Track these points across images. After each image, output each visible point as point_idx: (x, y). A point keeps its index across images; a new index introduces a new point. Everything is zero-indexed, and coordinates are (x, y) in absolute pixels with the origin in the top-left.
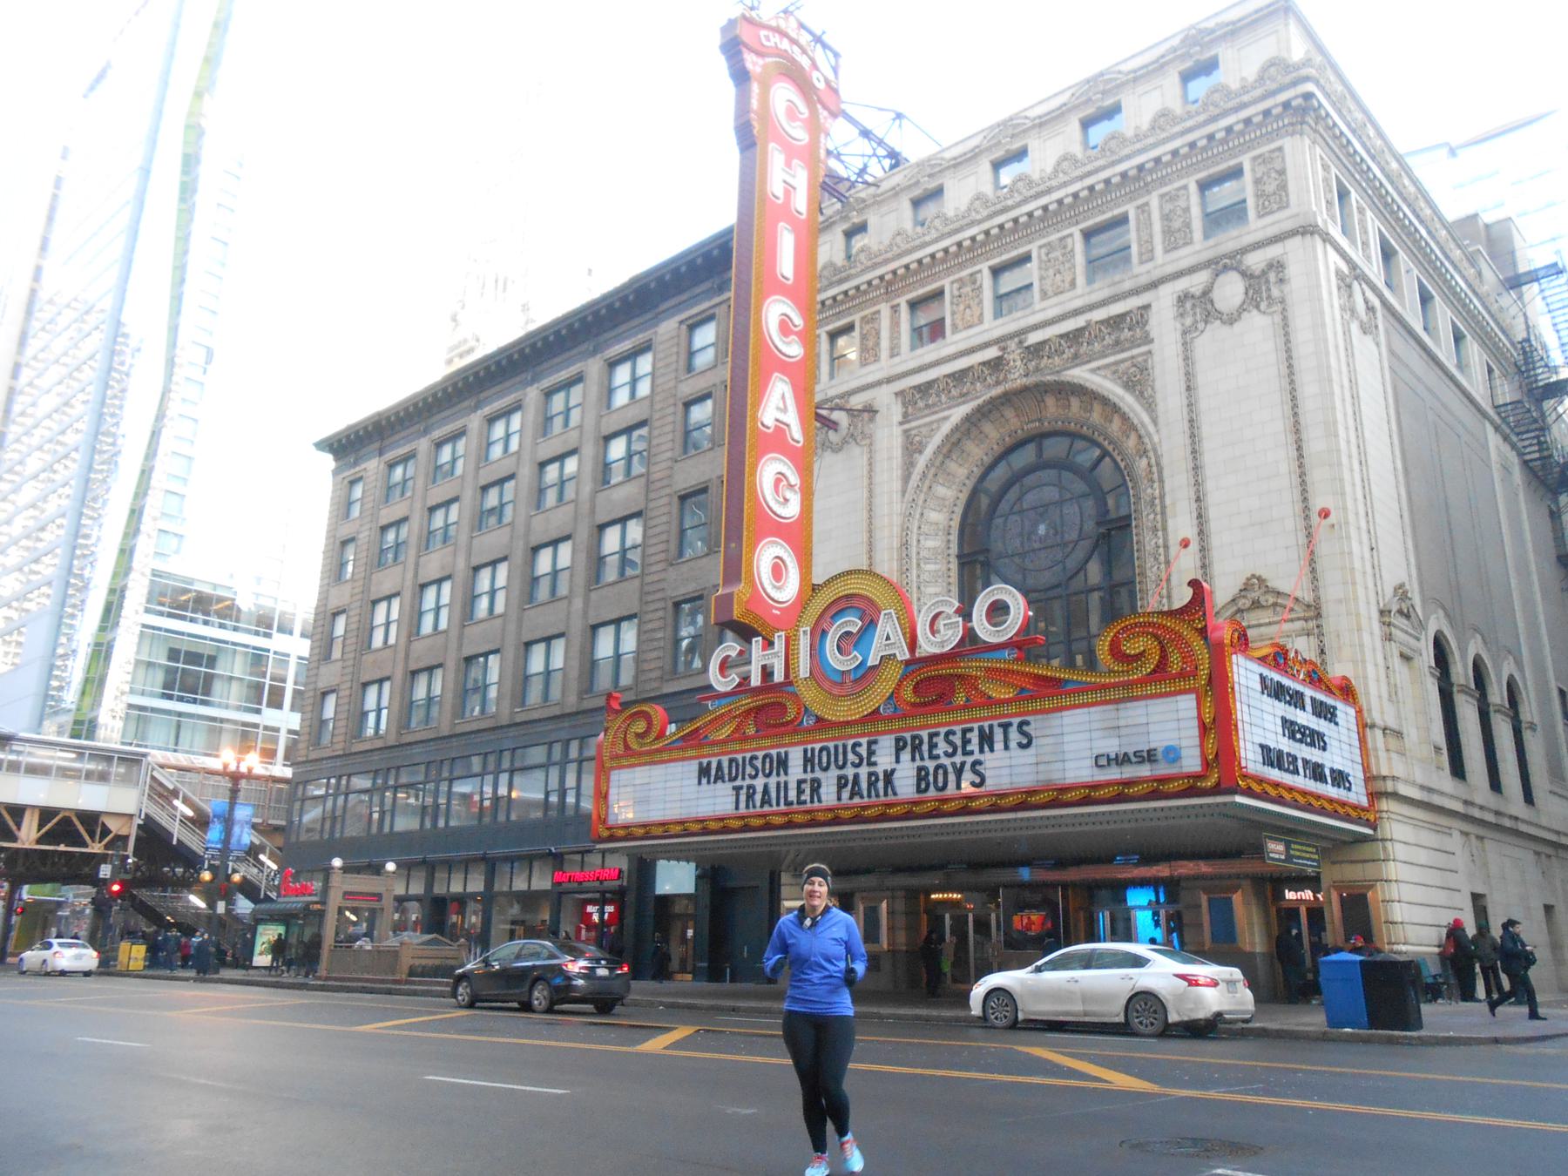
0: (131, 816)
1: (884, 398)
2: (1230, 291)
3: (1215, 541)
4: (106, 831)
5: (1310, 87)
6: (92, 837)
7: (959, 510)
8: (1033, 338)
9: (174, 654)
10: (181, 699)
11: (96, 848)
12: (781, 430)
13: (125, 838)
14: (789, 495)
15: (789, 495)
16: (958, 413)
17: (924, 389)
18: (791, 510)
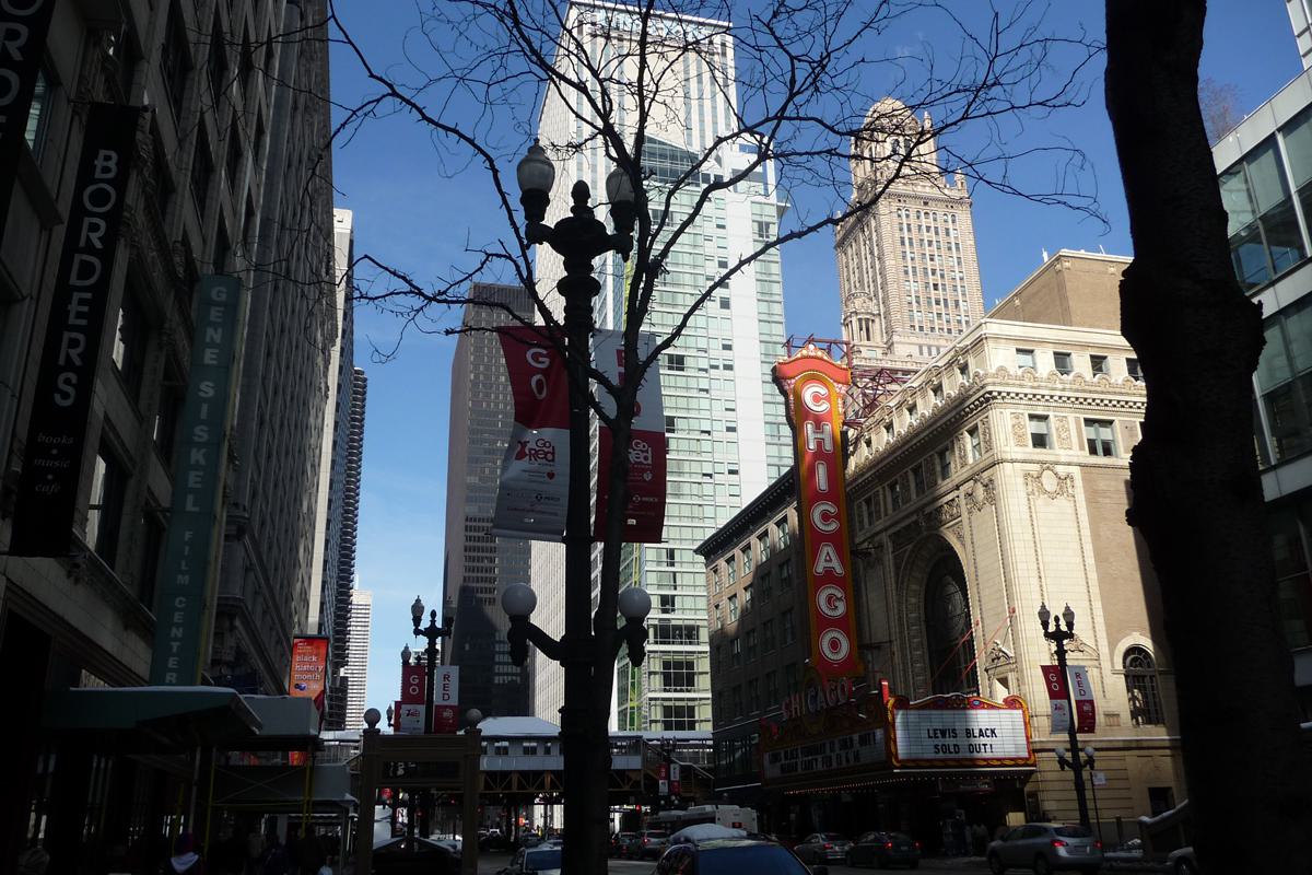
0: (639, 770)
1: (884, 537)
2: (980, 492)
3: (987, 622)
4: (629, 779)
5: (989, 388)
6: (623, 781)
7: (922, 596)
8: (927, 510)
9: (666, 665)
10: (676, 691)
11: (626, 788)
12: (829, 572)
13: (638, 782)
14: (837, 604)
15: (837, 604)
16: (910, 546)
17: (897, 534)
18: (841, 609)
